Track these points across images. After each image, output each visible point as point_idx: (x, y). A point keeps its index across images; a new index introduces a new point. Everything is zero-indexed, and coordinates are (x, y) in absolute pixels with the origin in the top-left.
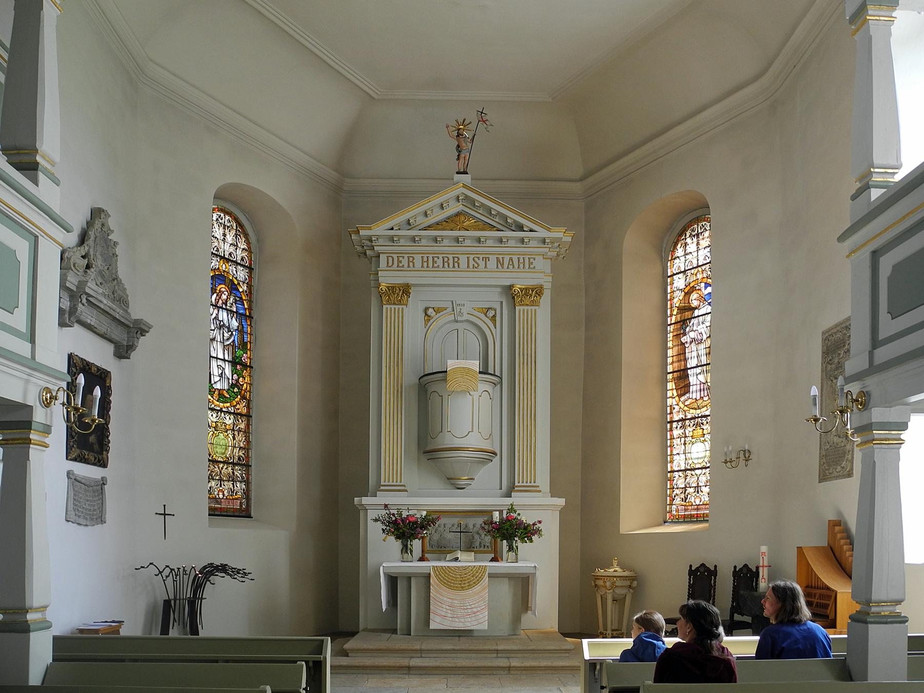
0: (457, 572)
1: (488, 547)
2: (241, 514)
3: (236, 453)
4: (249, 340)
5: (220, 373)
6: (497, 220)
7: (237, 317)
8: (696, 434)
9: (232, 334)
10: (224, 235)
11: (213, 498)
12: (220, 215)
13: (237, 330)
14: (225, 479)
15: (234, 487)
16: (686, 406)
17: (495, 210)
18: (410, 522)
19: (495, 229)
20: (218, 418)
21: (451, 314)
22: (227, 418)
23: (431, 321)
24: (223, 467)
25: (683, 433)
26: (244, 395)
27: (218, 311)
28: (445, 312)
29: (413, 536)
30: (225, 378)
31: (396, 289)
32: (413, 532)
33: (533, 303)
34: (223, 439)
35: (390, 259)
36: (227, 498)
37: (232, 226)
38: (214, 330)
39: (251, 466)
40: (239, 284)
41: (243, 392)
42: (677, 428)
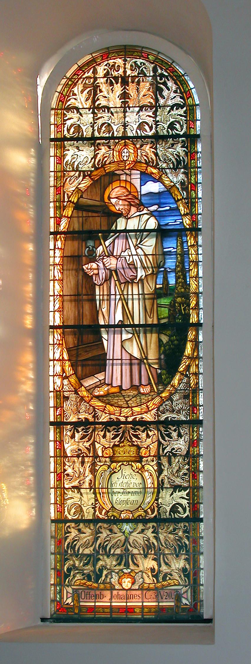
14: (167, 552)
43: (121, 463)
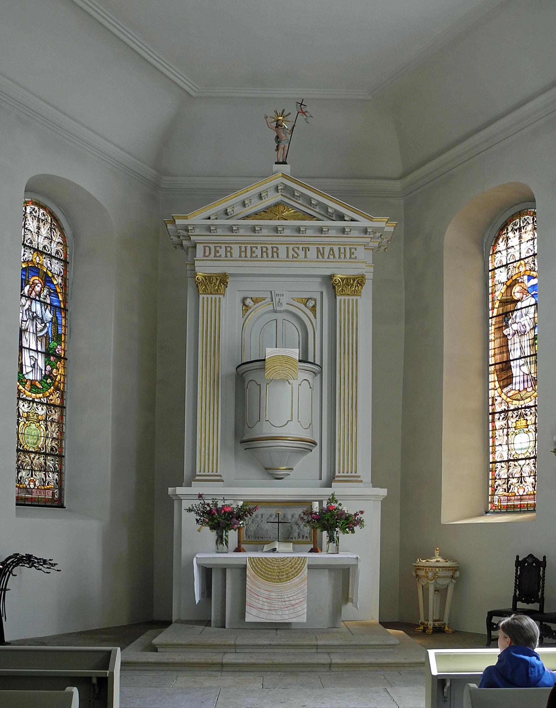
0: (275, 564)
1: (307, 537)
2: (53, 504)
3: (48, 443)
4: (63, 332)
5: (32, 364)
6: (317, 210)
7: (51, 309)
8: (520, 425)
9: (45, 326)
10: (39, 228)
11: (23, 488)
12: (34, 209)
13: (51, 321)
15: (46, 478)
16: (509, 397)
17: (315, 199)
18: (225, 512)
19: (315, 219)
20: (29, 408)
21: (270, 304)
22: (40, 408)
23: (250, 311)
24: (35, 457)
25: (505, 425)
26: (58, 386)
27: (31, 302)
28: (263, 302)
29: (229, 527)
30: (37, 369)
31: (213, 279)
32: (228, 523)
33: (355, 293)
34: (35, 430)
35: (207, 249)
36: (38, 488)
37: (46, 219)
38: (26, 321)
39: (64, 456)
40: (53, 276)
41: (57, 383)
42: (499, 419)
43: (31, 422)
